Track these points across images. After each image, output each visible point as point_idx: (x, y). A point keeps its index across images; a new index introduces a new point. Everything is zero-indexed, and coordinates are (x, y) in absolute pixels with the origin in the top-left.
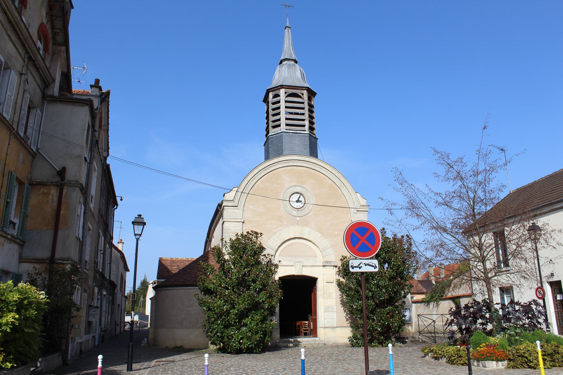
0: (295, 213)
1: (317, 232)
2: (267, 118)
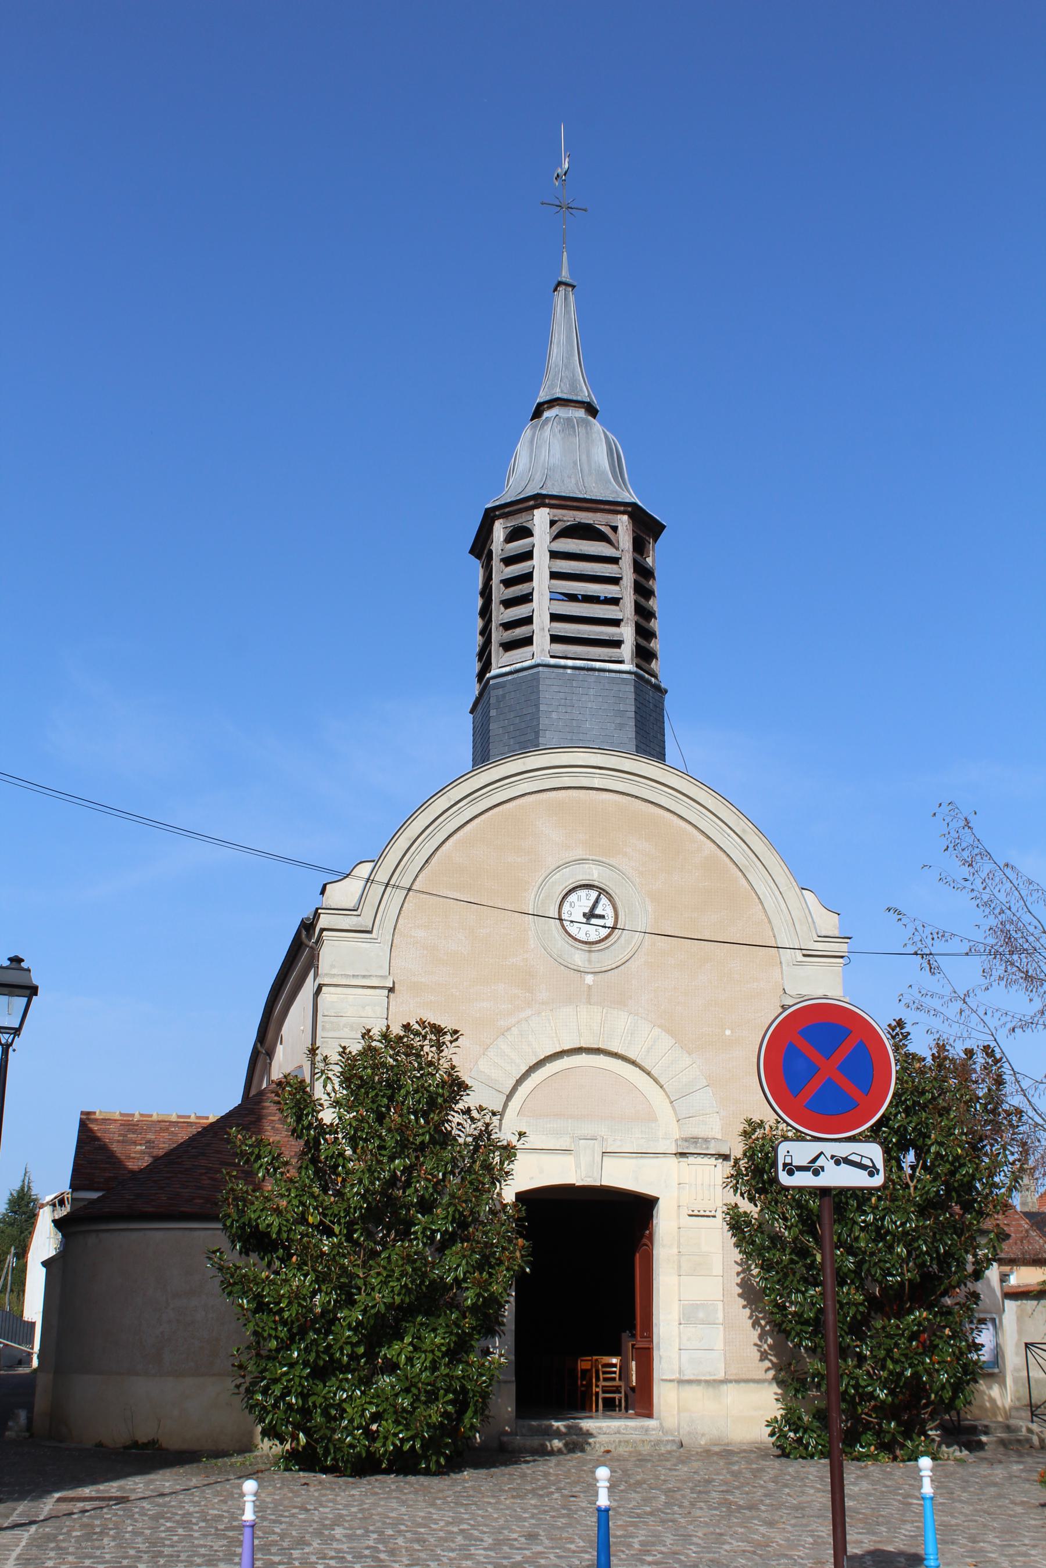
0: (579, 958)
1: (657, 1031)
2: (485, 612)
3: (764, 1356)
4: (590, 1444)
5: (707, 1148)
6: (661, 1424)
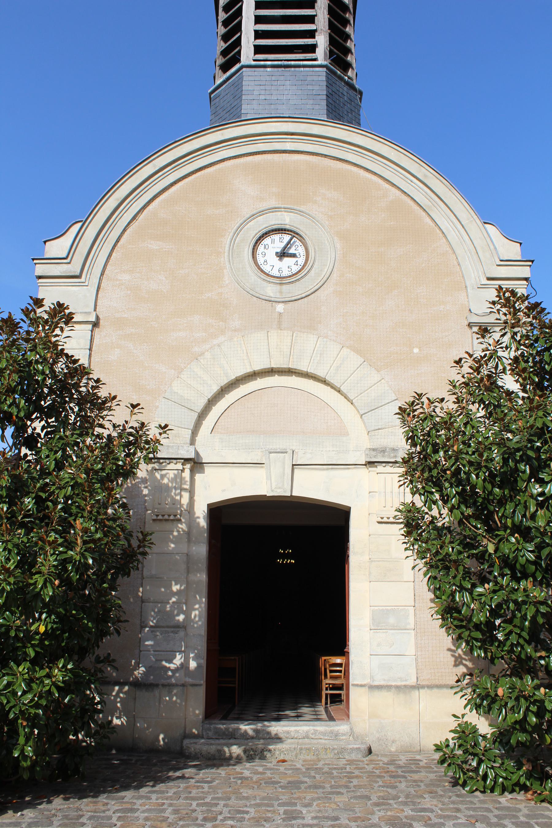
0: (271, 290)
1: (346, 351)
3: (458, 662)
4: (270, 751)
6: (351, 729)
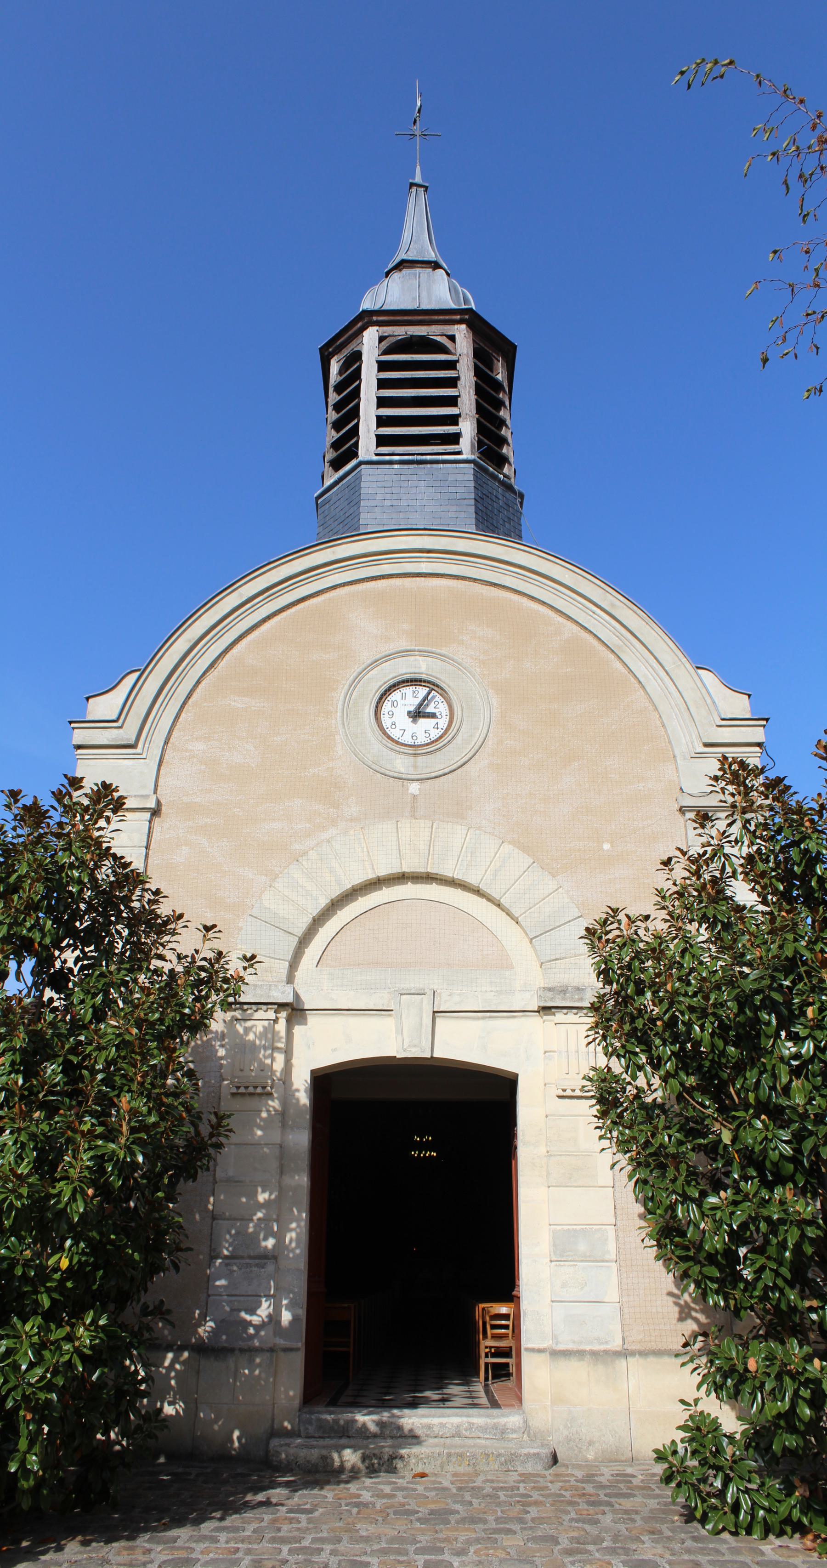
0: (401, 764)
1: (507, 848)
3: (684, 1314)
4: (402, 1457)
5: (581, 999)
6: (525, 1422)
